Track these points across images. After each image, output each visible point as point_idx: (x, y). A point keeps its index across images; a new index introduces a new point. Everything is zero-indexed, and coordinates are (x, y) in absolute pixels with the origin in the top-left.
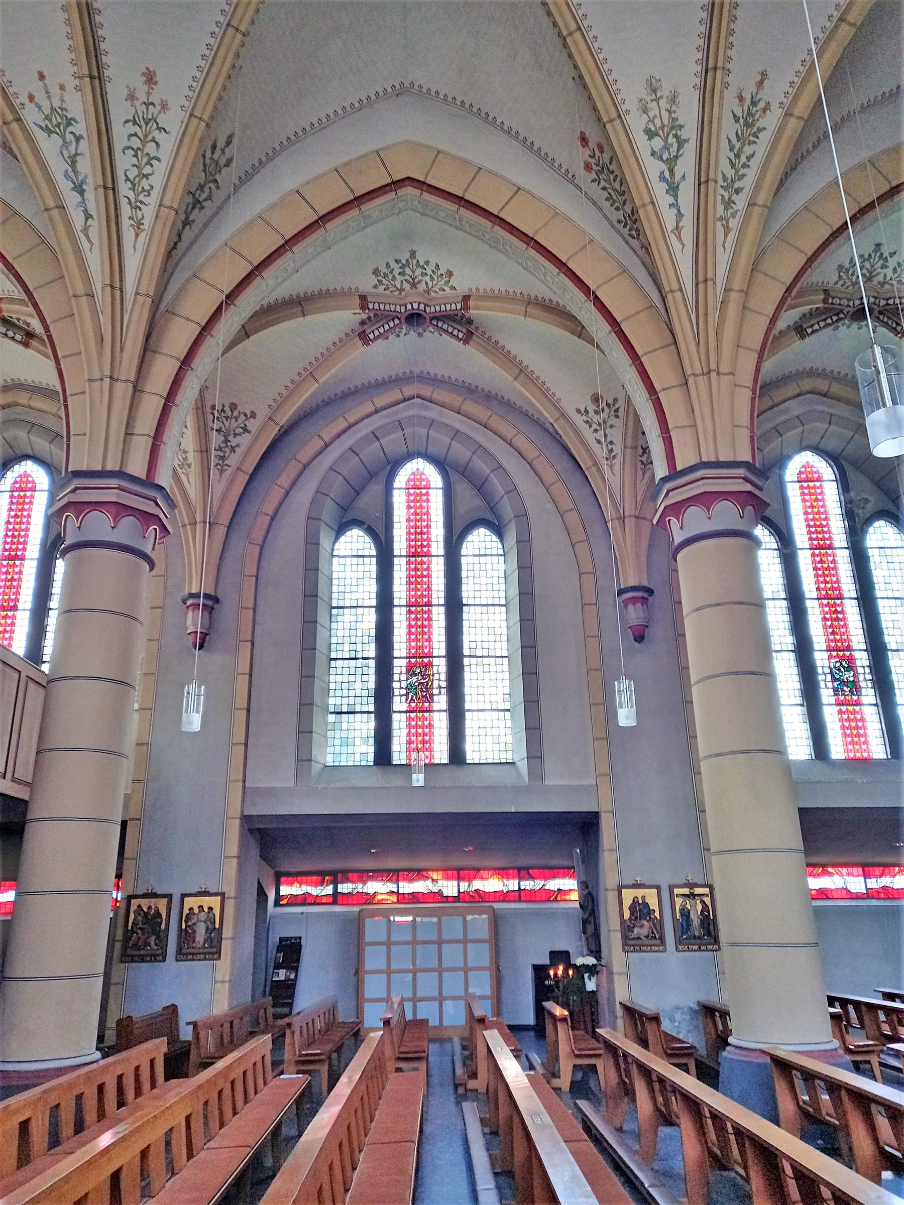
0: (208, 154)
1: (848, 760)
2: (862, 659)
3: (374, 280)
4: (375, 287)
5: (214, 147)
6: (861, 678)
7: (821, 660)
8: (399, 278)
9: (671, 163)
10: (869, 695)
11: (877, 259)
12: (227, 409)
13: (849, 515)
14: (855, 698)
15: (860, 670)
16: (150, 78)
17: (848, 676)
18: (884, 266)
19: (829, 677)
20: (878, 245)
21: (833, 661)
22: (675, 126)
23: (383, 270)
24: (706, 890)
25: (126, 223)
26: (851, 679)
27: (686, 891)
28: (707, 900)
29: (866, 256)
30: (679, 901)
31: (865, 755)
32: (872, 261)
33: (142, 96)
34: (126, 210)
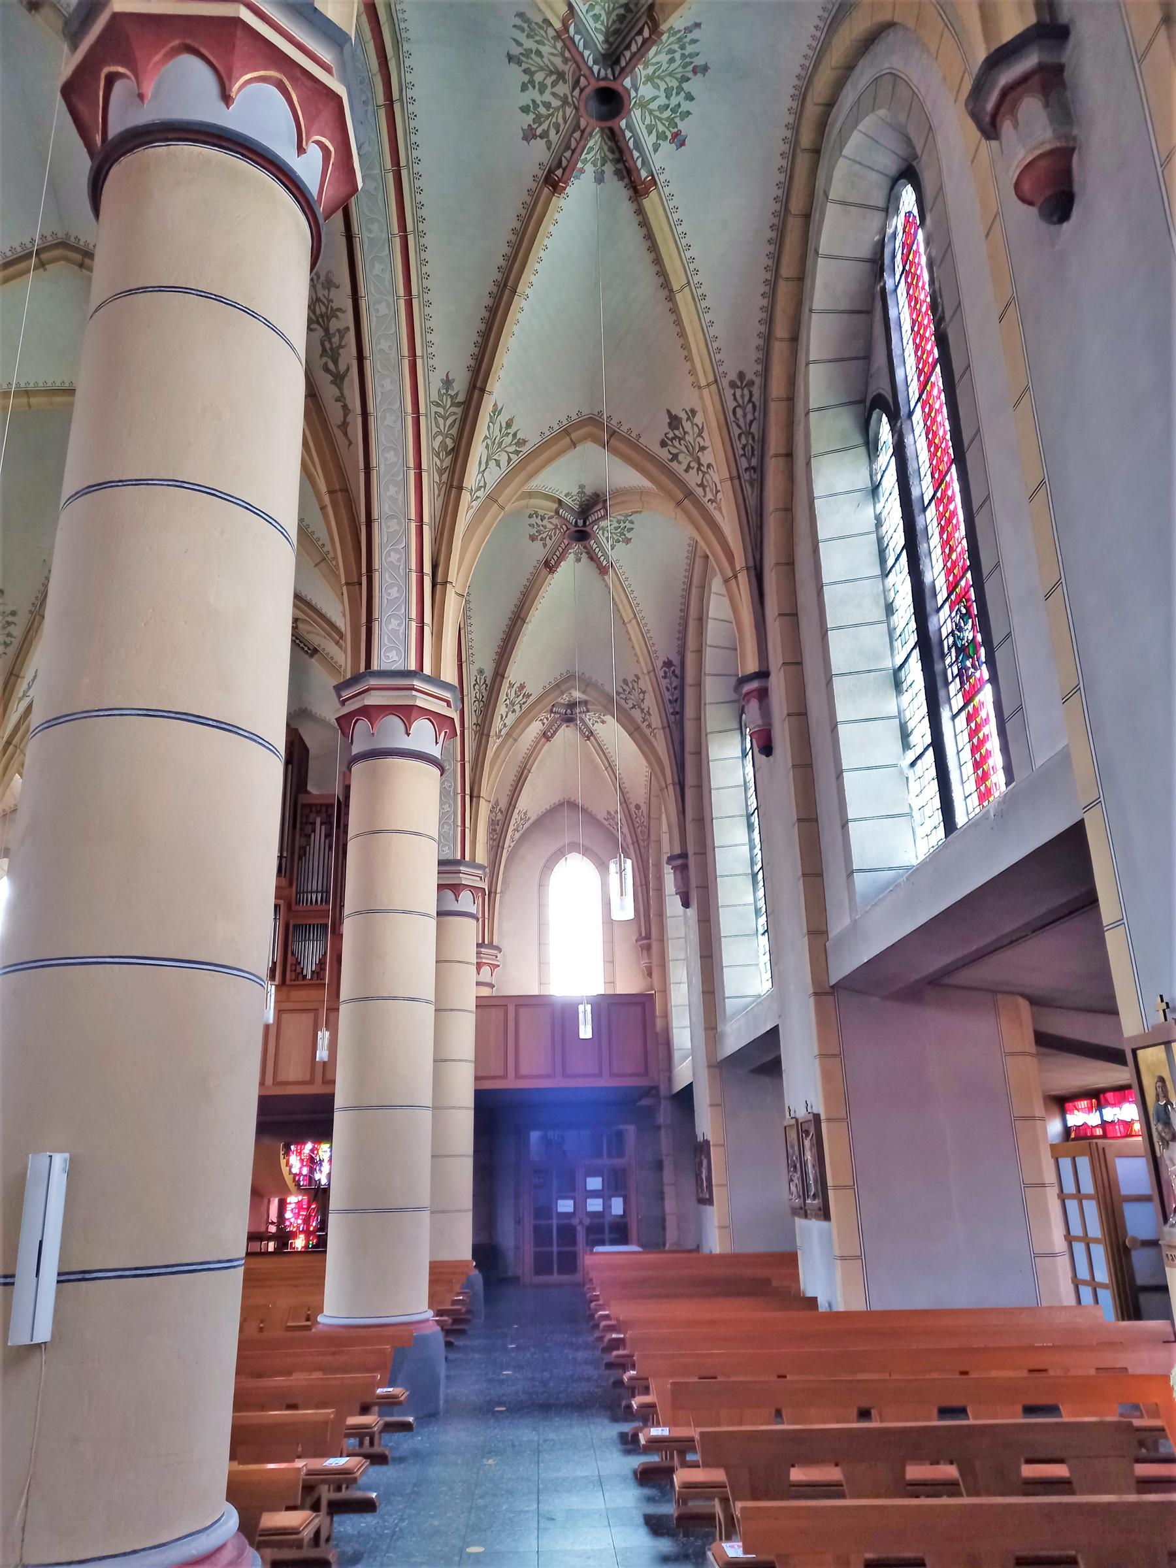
3: (538, 544)
4: (545, 545)
8: (545, 522)
11: (530, 61)
12: (625, 687)
18: (539, 53)
20: (510, 58)
23: (533, 531)
29: (526, 78)
32: (533, 69)
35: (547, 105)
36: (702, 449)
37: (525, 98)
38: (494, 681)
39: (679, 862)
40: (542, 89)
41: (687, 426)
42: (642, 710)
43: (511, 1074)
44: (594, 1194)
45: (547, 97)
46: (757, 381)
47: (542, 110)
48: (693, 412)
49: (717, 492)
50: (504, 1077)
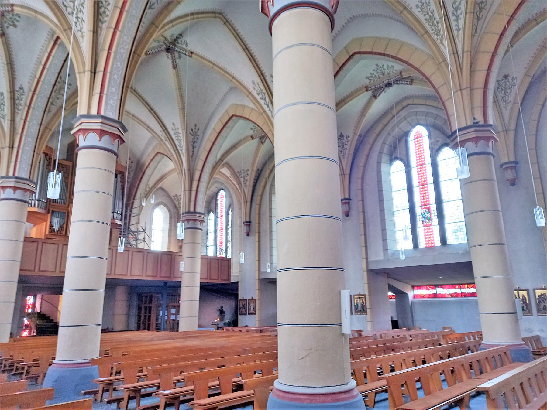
0: (191, 132)
1: (426, 247)
2: (434, 208)
3: (252, 131)
5: (192, 130)
6: (433, 215)
7: (419, 210)
9: (265, 99)
10: (435, 221)
13: (431, 149)
14: (430, 223)
15: (432, 212)
16: (174, 124)
17: (428, 215)
19: (421, 216)
21: (423, 210)
22: (262, 90)
24: (363, 296)
25: (181, 155)
26: (429, 216)
27: (358, 297)
28: (364, 299)
30: (356, 299)
31: (433, 245)
33: (174, 128)
34: (180, 152)
35: (375, 76)
36: (346, 144)
37: (372, 72)
38: (219, 161)
39: (248, 223)
40: (378, 73)
41: (345, 138)
42: (244, 179)
43: (113, 274)
44: (173, 314)
45: (377, 75)
46: (363, 136)
47: (374, 76)
48: (349, 137)
49: (345, 154)
50: (126, 275)
